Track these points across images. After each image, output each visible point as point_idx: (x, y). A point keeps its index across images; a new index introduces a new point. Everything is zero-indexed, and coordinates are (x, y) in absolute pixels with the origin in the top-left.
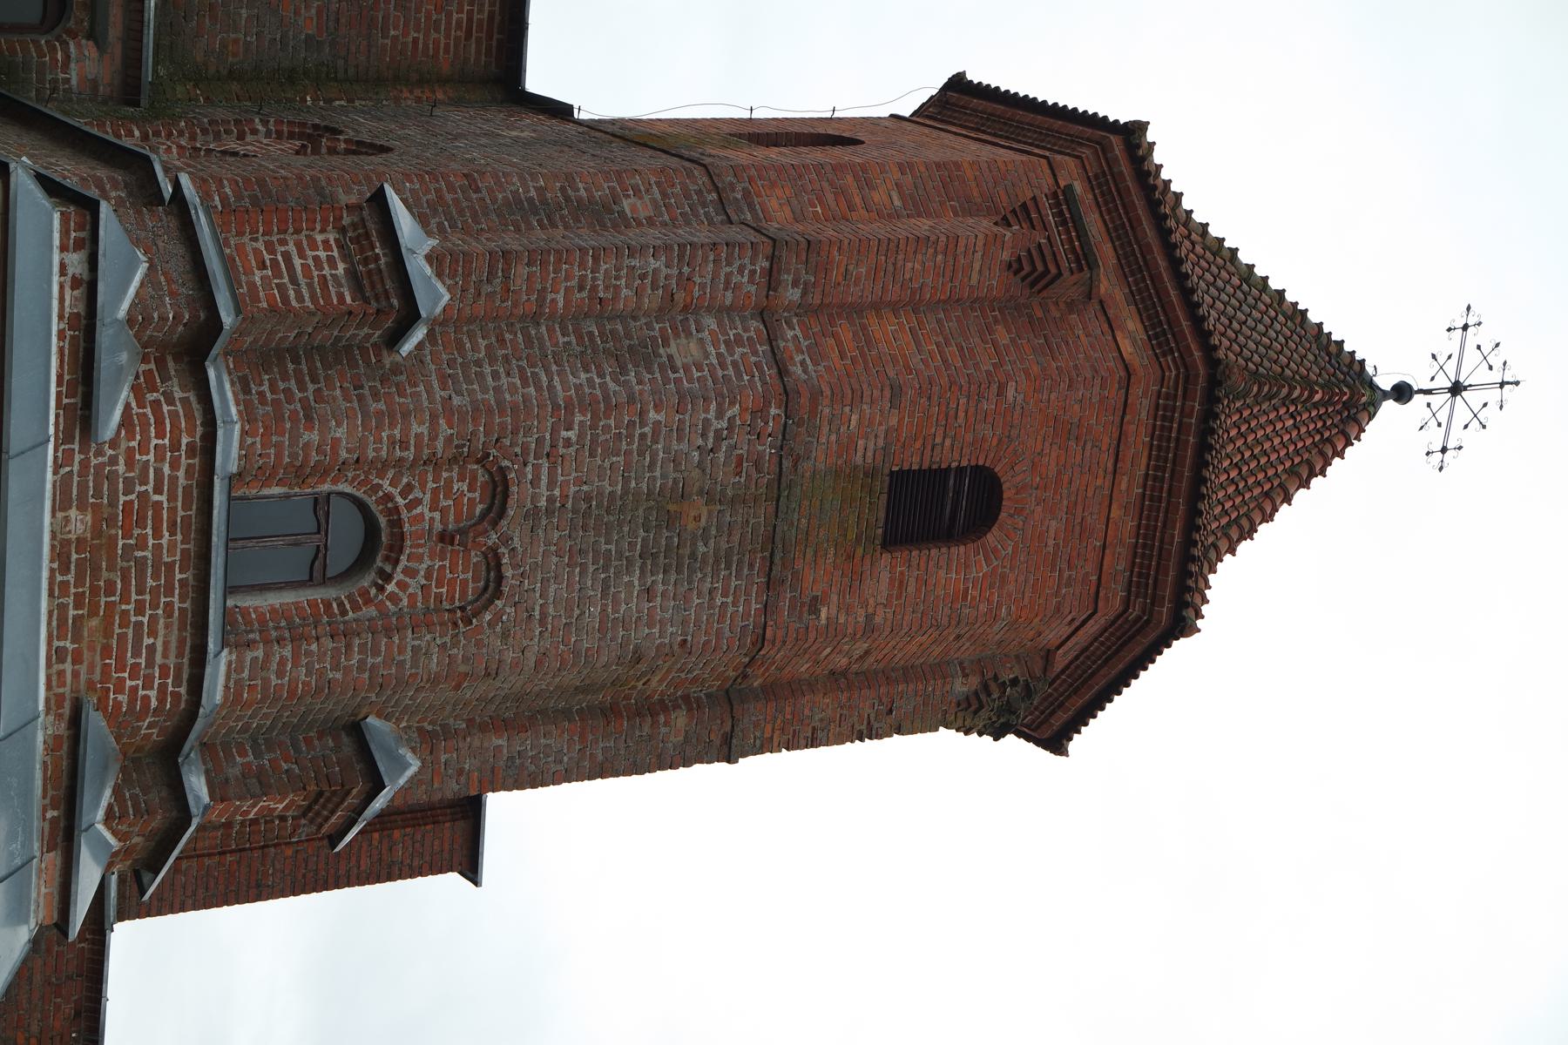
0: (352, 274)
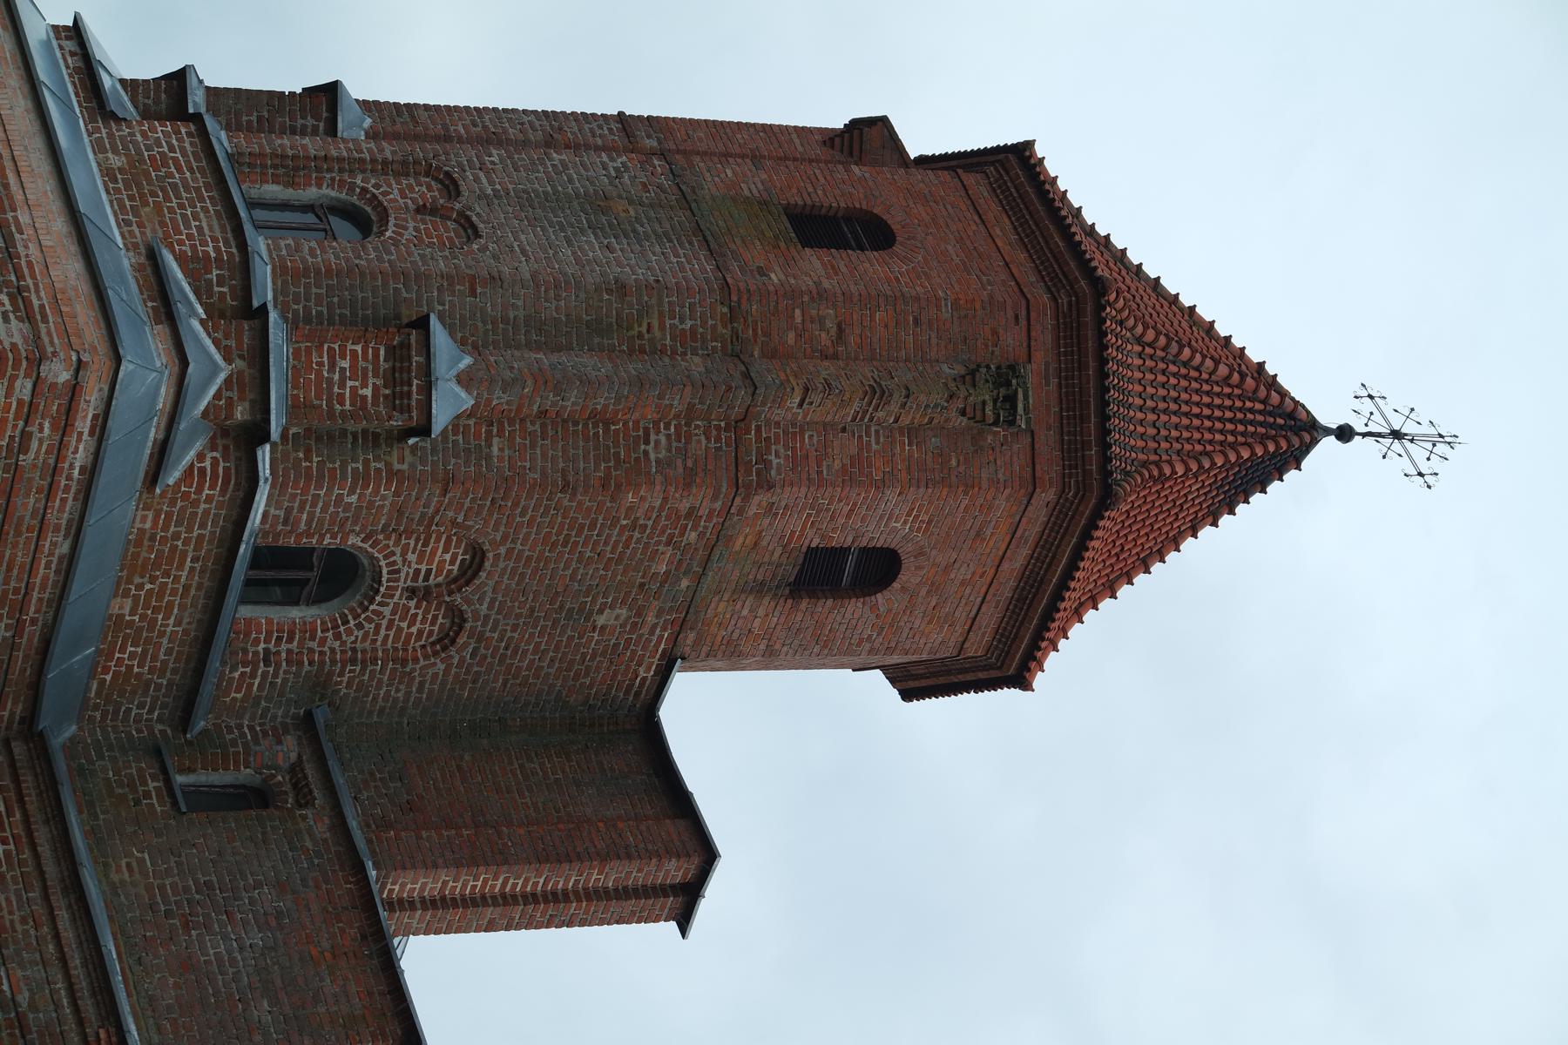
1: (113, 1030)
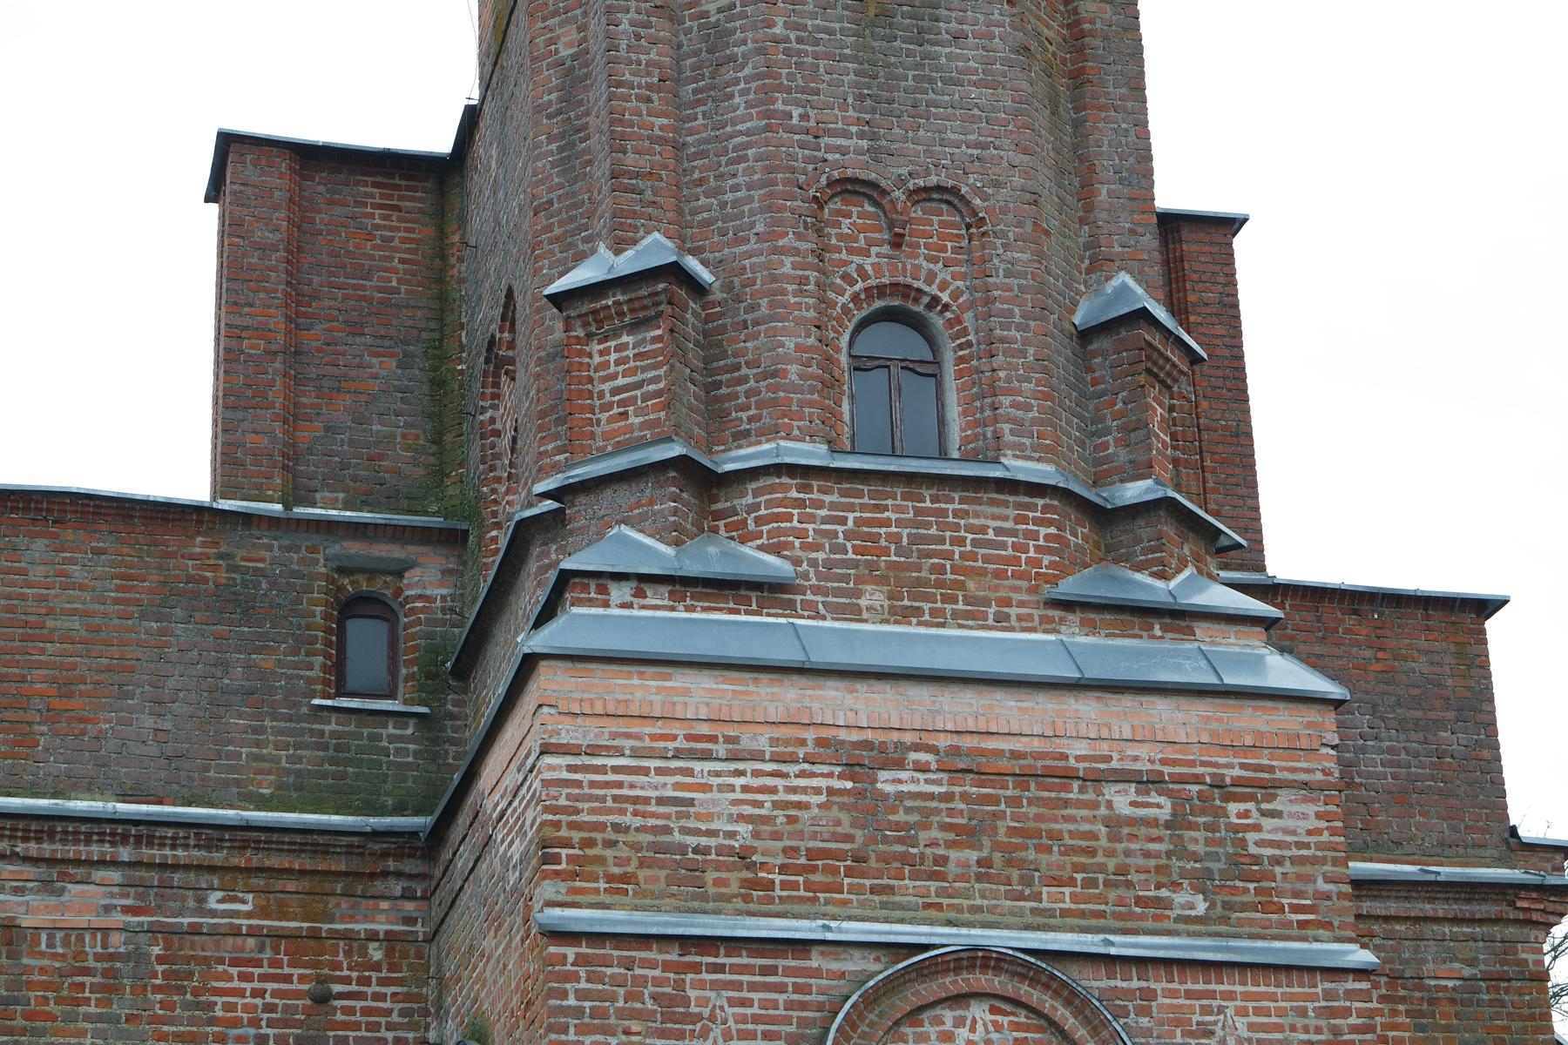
0: (633, 328)
1: (1523, 894)
